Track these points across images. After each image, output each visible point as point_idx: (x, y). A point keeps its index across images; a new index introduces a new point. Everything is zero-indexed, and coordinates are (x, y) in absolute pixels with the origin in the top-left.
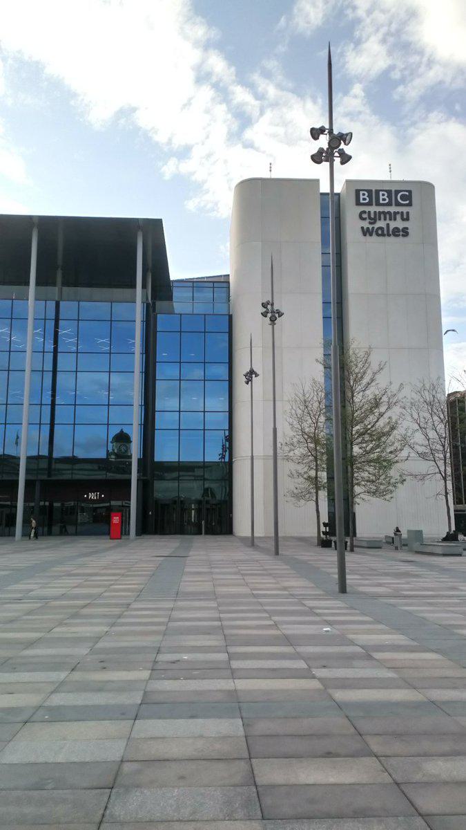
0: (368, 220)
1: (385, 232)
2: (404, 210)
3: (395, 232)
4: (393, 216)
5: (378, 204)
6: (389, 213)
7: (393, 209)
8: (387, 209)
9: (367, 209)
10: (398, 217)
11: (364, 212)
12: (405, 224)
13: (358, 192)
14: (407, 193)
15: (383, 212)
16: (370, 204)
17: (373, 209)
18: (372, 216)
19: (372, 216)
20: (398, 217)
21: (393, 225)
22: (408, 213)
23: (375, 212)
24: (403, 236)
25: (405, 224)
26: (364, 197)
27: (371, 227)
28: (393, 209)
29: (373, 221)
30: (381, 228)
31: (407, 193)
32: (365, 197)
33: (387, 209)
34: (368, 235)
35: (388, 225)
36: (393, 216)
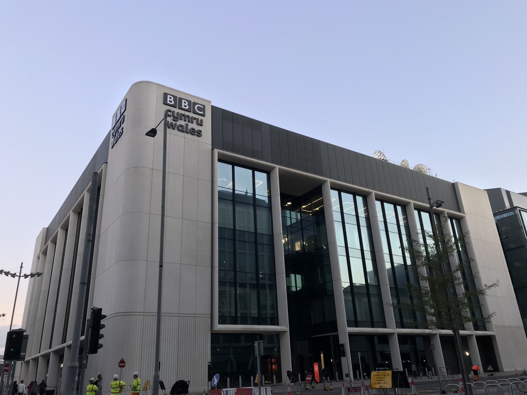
0: (172, 118)
1: (185, 129)
2: (200, 118)
3: (193, 132)
4: (191, 120)
5: (181, 108)
6: (188, 116)
7: (191, 115)
8: (187, 113)
9: (172, 109)
10: (195, 121)
11: (170, 111)
12: (200, 128)
13: (165, 95)
14: (202, 107)
15: (184, 115)
16: (174, 106)
17: (176, 110)
18: (176, 115)
19: (176, 115)
20: (195, 121)
21: (191, 126)
22: (202, 121)
23: (178, 113)
24: (197, 136)
25: (200, 128)
26: (170, 100)
27: (174, 122)
28: (191, 115)
29: (175, 119)
30: (181, 126)
31: (202, 107)
32: (172, 100)
33: (187, 113)
34: (171, 128)
35: (187, 125)
36: (191, 120)
